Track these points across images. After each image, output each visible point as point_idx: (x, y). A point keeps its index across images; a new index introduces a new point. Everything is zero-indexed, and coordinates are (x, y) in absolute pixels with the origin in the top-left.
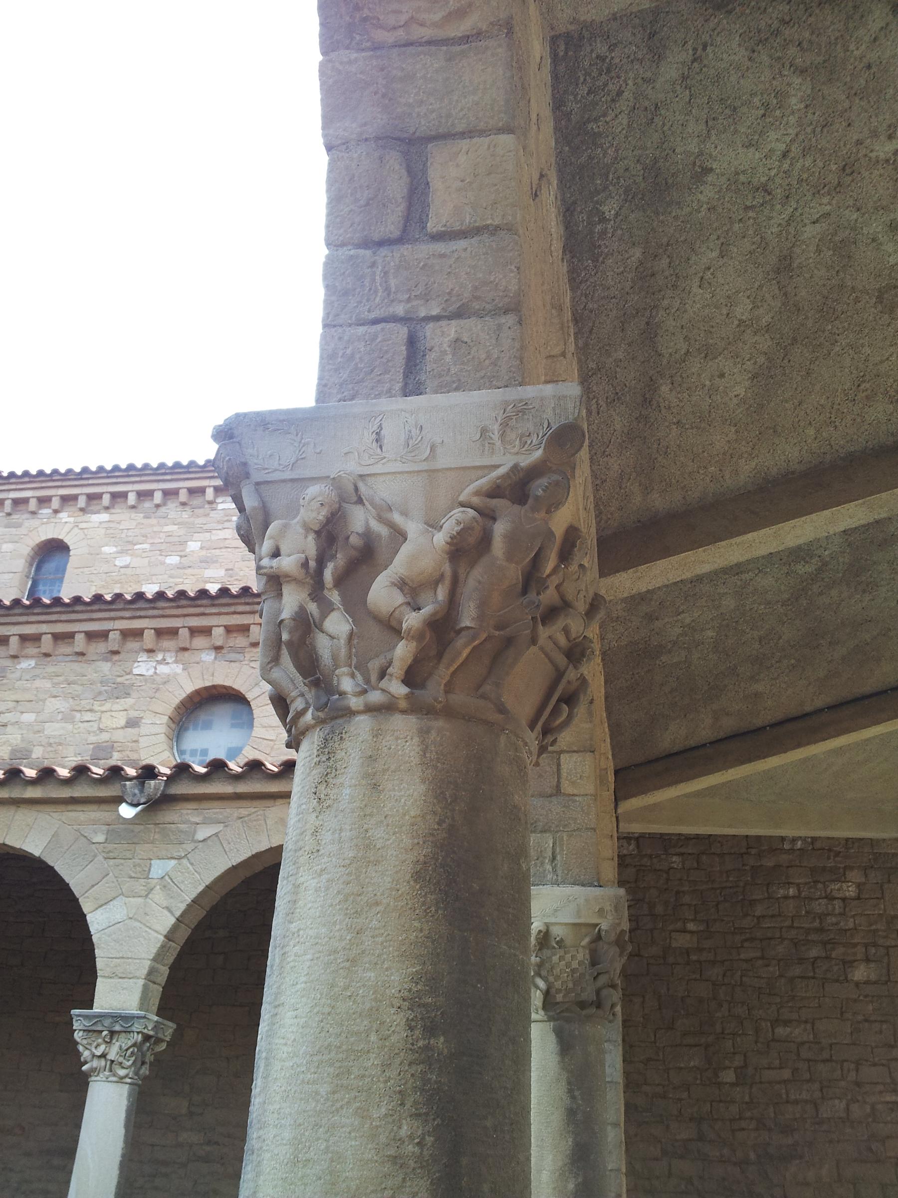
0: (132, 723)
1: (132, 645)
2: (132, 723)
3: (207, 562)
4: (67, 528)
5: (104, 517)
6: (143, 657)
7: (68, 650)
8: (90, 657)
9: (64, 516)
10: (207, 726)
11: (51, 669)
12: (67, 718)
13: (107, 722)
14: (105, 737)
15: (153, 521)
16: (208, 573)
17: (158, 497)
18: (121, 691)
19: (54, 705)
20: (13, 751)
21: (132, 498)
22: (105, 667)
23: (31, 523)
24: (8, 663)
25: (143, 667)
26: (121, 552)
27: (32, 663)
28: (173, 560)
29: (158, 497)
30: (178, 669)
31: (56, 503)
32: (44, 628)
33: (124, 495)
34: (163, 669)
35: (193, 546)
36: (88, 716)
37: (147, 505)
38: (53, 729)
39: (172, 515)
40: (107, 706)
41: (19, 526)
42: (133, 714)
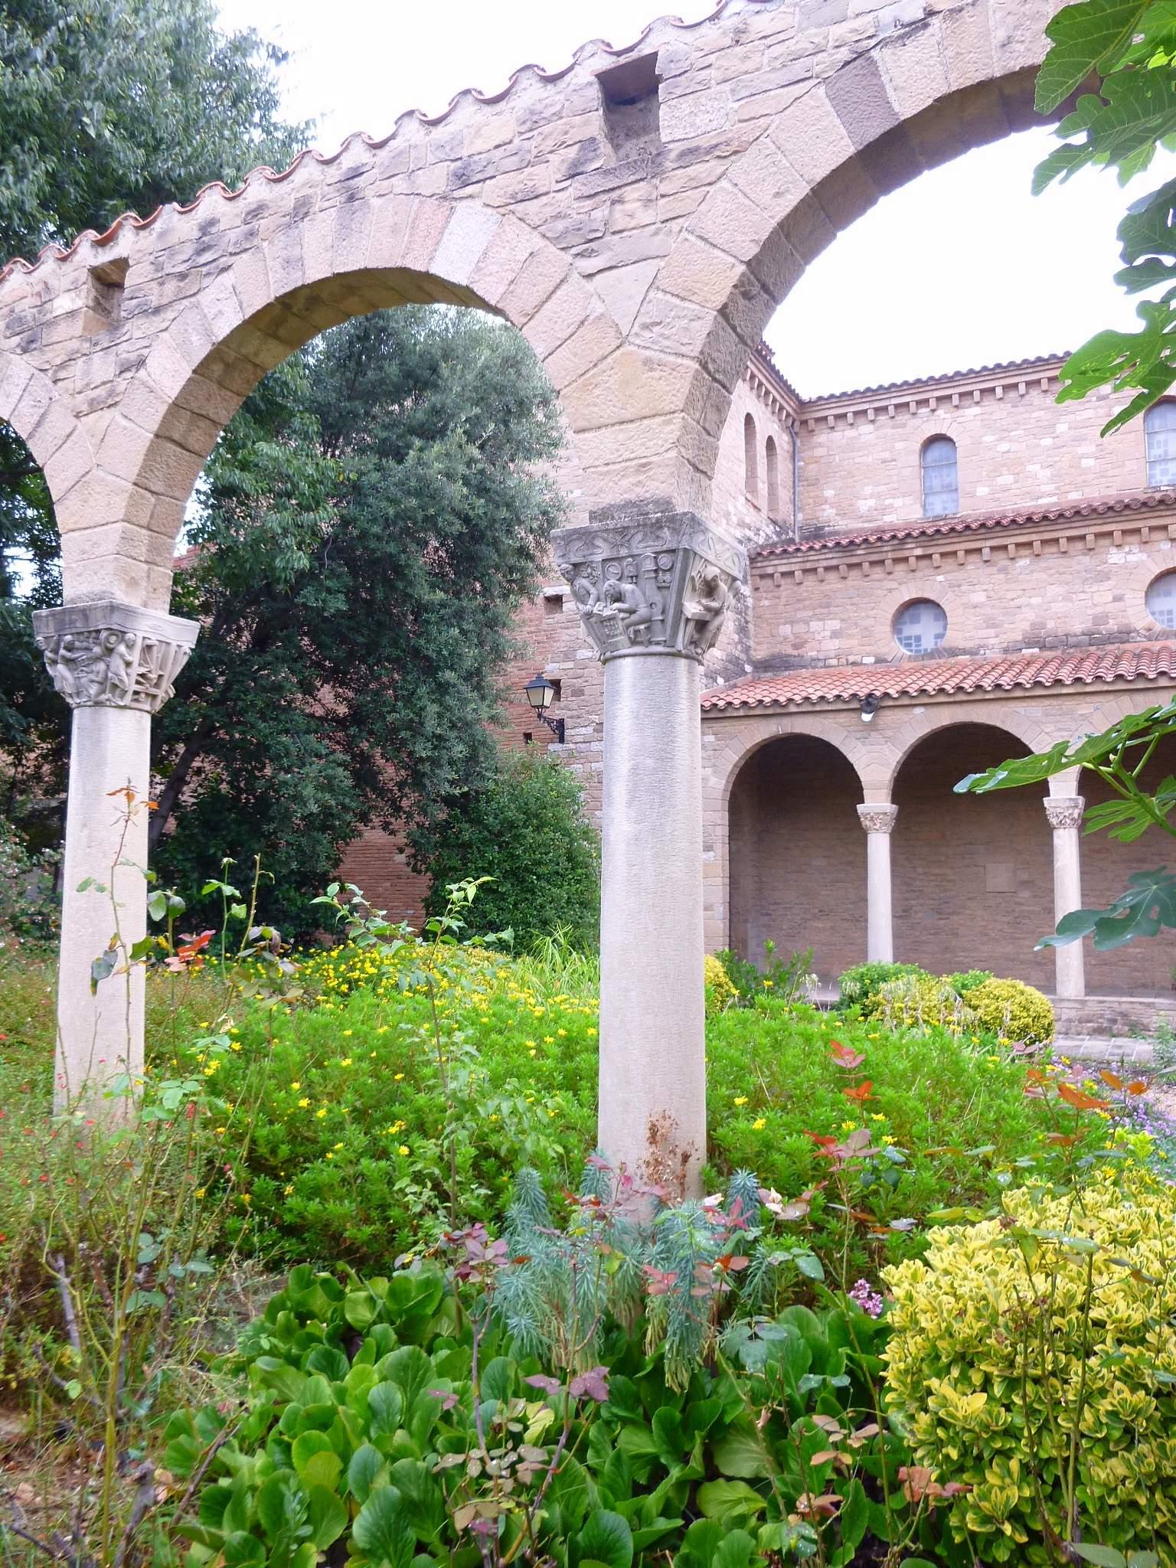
0: (1118, 599)
1: (1106, 542)
2: (1118, 599)
3: (1079, 440)
4: (947, 423)
5: (976, 410)
6: (1113, 550)
7: (1054, 549)
8: (1072, 552)
9: (940, 412)
10: (1168, 594)
11: (1043, 564)
12: (1067, 598)
13: (1097, 599)
14: (1099, 609)
15: (1021, 409)
16: (1081, 450)
17: (1022, 388)
18: (1105, 577)
19: (1053, 590)
20: (1033, 625)
21: (999, 391)
22: (1086, 560)
23: (916, 422)
24: (1007, 563)
25: (1115, 557)
26: (1001, 439)
27: (1027, 561)
28: (1047, 441)
29: (1022, 388)
30: (1144, 556)
31: (933, 403)
32: (1034, 537)
33: (993, 390)
34: (1130, 558)
35: (1062, 428)
36: (1082, 596)
37: (1012, 394)
38: (1059, 607)
39: (1036, 402)
40: (1095, 588)
41: (904, 426)
42: (1118, 592)
